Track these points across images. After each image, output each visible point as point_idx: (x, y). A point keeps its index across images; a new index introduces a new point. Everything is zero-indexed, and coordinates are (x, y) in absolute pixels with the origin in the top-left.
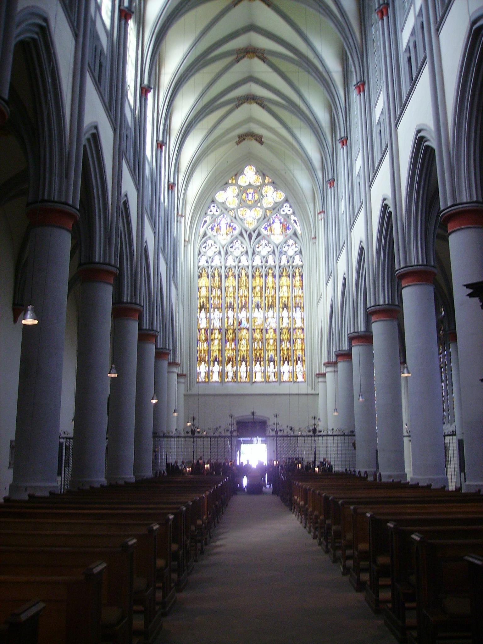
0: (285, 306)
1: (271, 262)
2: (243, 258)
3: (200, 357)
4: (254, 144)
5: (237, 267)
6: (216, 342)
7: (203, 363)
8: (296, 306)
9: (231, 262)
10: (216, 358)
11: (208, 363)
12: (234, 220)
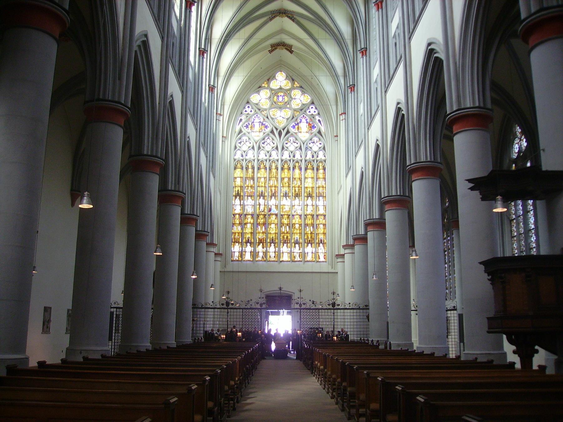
0: (310, 196)
1: (298, 156)
2: (274, 153)
3: (234, 238)
4: (285, 52)
5: (268, 161)
6: (249, 226)
7: (237, 244)
8: (319, 195)
9: (262, 156)
10: (248, 240)
11: (242, 245)
12: (266, 119)
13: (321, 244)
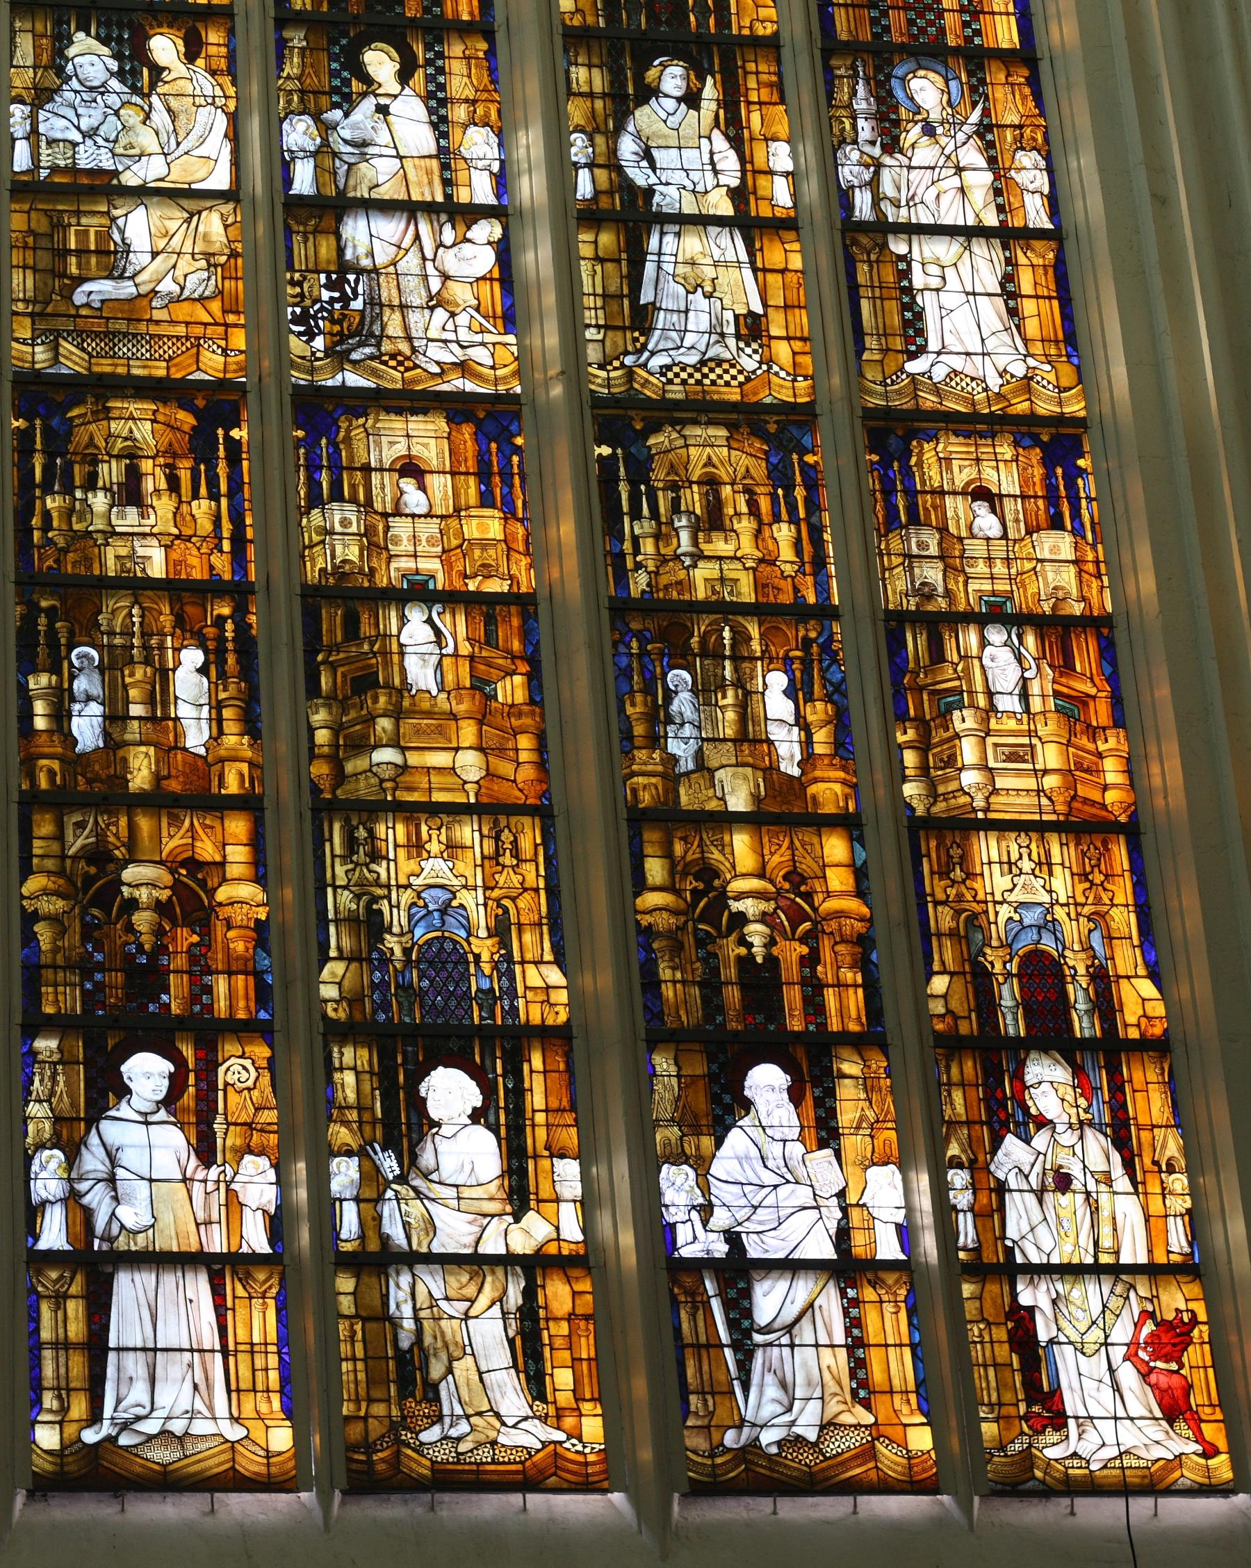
13: (1048, 1084)
